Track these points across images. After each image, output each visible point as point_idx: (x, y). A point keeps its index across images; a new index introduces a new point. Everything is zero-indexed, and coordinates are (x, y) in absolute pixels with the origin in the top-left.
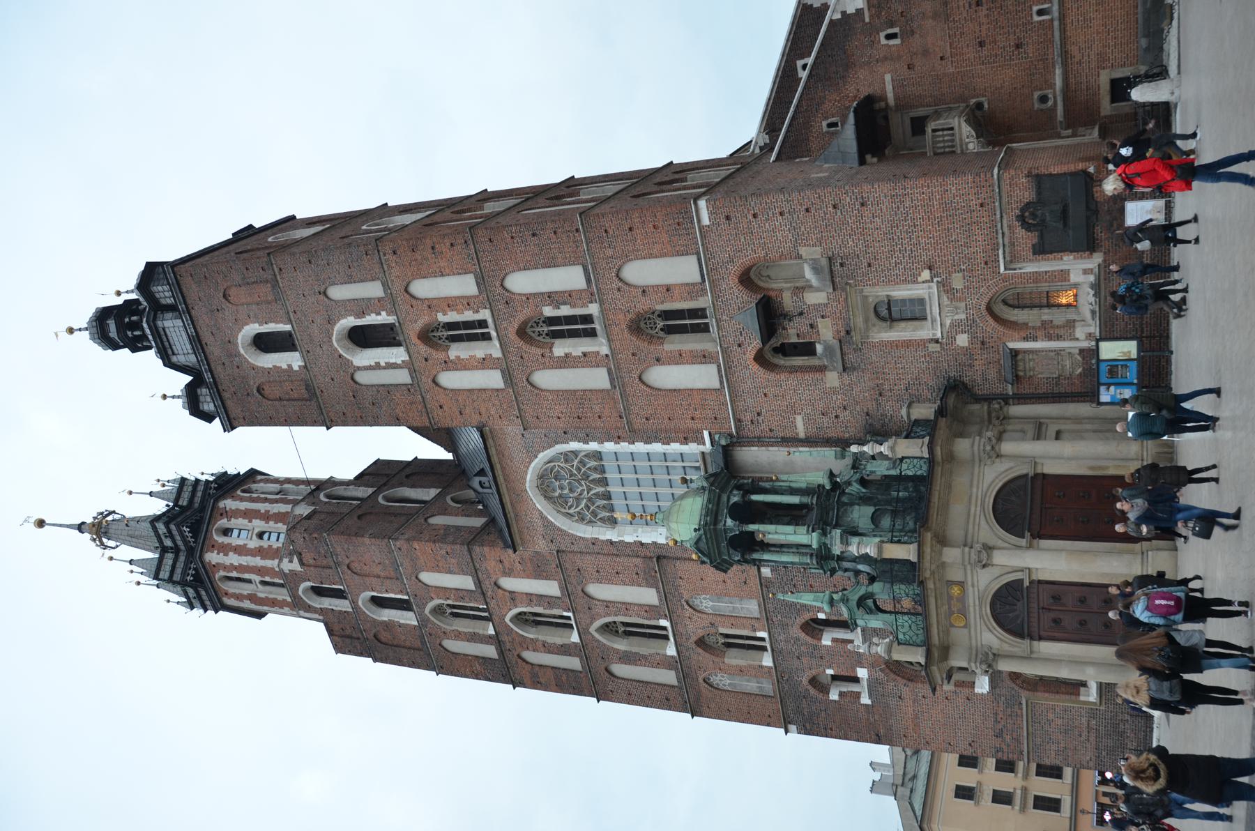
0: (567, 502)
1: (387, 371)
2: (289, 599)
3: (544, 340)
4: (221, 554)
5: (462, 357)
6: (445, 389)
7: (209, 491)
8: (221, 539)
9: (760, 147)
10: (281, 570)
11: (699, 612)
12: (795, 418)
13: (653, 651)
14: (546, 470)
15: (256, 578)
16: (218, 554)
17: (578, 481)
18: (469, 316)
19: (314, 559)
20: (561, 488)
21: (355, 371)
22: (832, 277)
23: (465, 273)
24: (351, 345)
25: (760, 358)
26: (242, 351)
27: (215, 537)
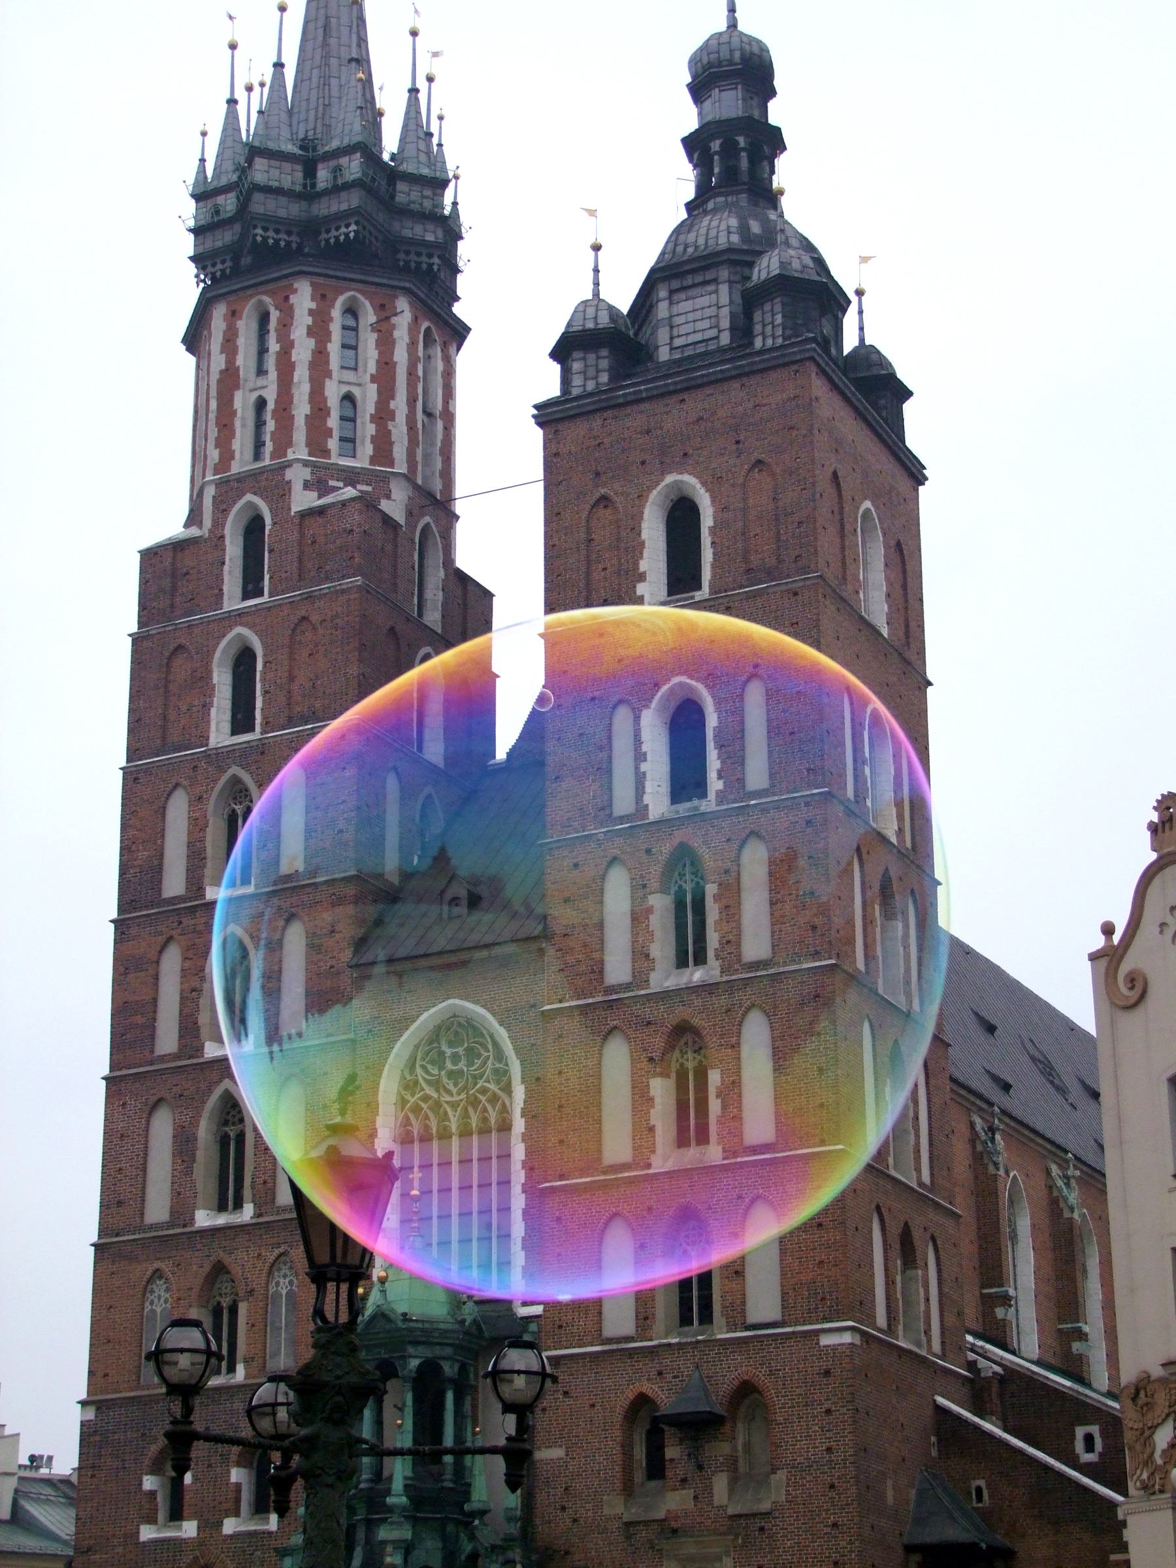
0: (433, 1062)
1: (632, 770)
2: (236, 468)
3: (674, 1058)
4: (309, 320)
5: (651, 916)
6: (603, 878)
7: (424, 251)
8: (336, 313)
9: (975, 1362)
10: (289, 464)
11: (270, 1272)
12: (561, 1446)
13: (200, 1187)
14: (482, 1035)
15: (271, 396)
16: (311, 312)
17: (465, 1088)
18: (713, 939)
19: (314, 542)
20: (456, 1058)
21: (633, 709)
22: (746, 1515)
23: (773, 946)
24: (673, 705)
25: (642, 1401)
26: (670, 479)
27: (340, 301)
